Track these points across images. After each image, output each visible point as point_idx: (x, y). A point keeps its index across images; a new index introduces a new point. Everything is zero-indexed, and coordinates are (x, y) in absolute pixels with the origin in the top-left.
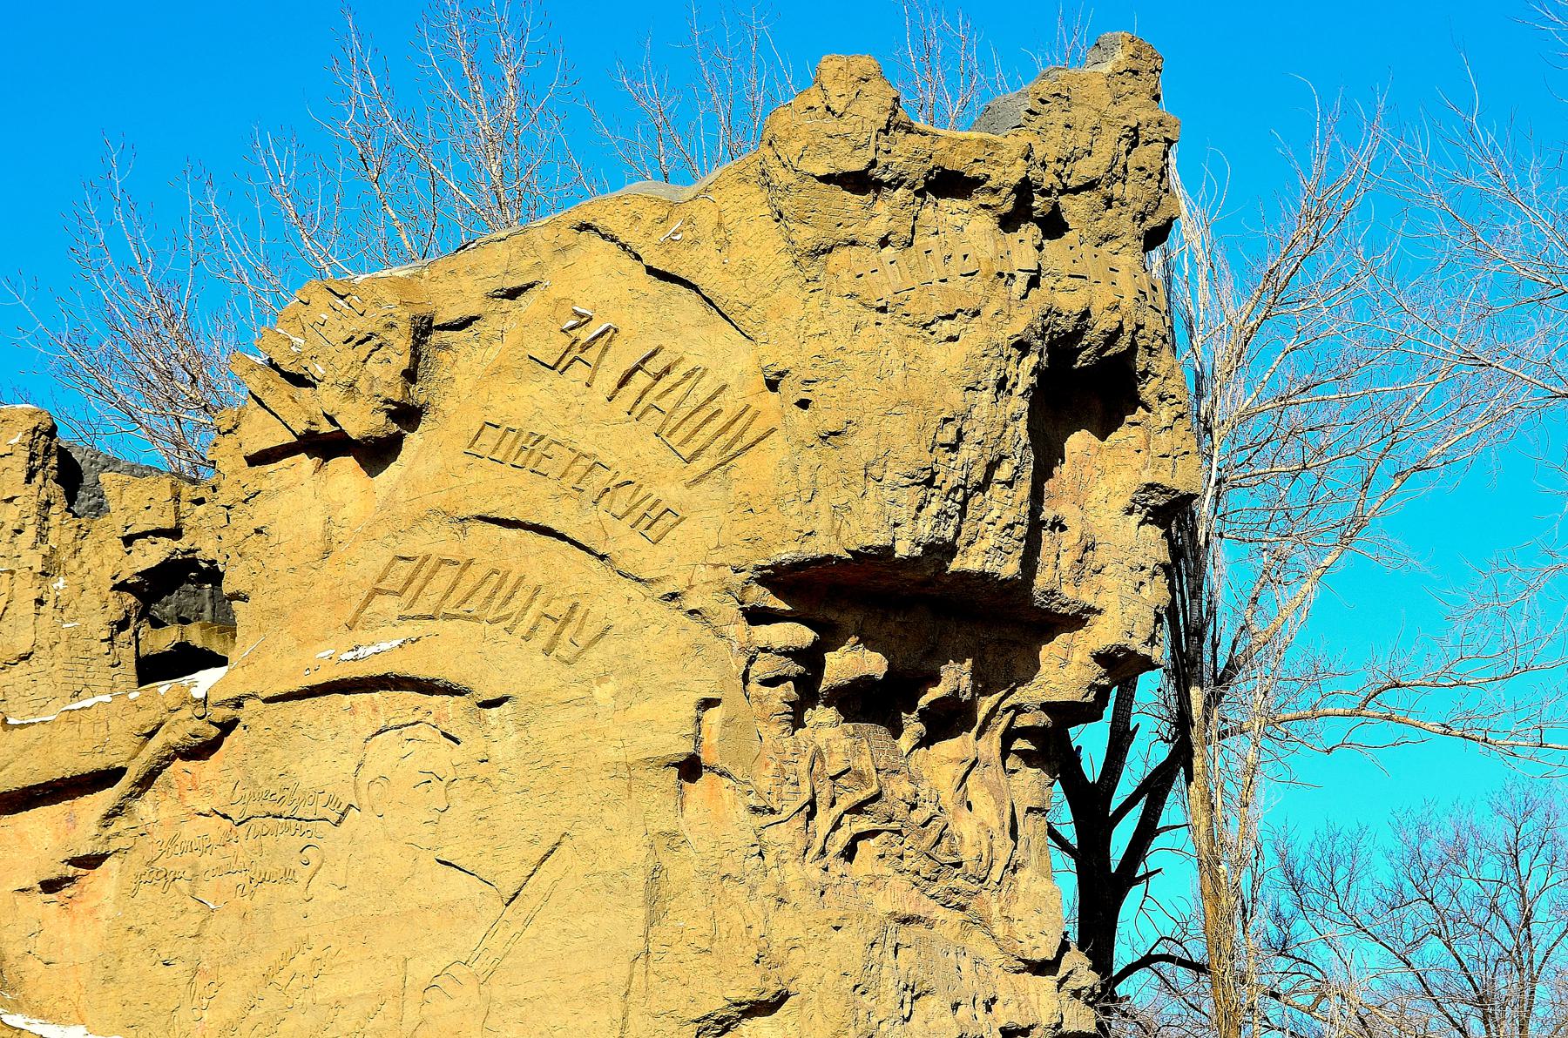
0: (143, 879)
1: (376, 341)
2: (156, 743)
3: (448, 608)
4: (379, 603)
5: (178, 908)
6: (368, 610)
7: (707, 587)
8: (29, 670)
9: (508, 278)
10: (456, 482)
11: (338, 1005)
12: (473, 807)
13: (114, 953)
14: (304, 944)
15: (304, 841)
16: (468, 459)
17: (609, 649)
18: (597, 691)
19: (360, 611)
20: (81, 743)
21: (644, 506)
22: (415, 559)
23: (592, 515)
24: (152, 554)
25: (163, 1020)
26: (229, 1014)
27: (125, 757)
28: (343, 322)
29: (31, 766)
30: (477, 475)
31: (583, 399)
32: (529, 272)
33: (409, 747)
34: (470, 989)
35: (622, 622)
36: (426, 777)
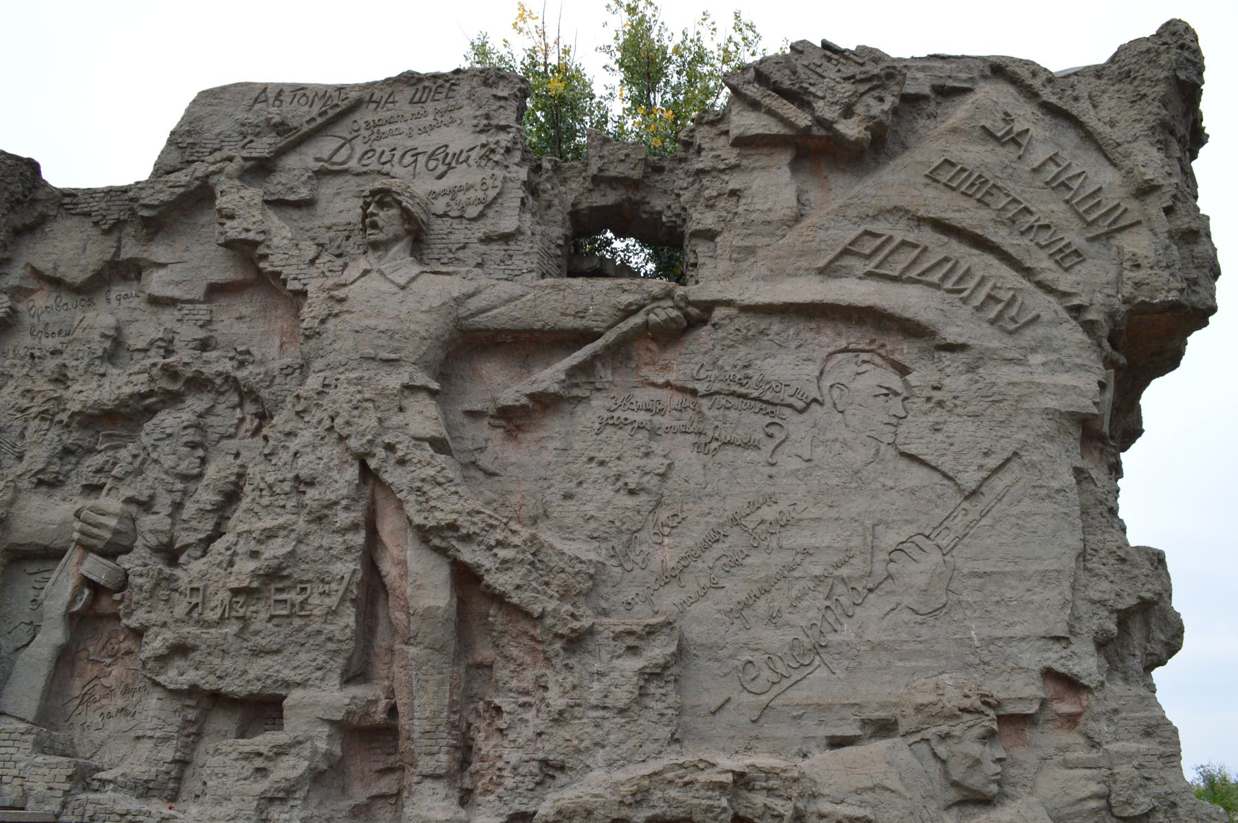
0: (610, 422)
1: (875, 83)
2: (638, 320)
3: (914, 274)
4: (848, 261)
5: (643, 449)
6: (837, 264)
7: (1103, 308)
8: (506, 247)
9: (951, 81)
10: (917, 193)
11: (806, 552)
12: (931, 419)
13: (574, 475)
14: (771, 500)
15: (768, 420)
16: (928, 181)
17: (1039, 331)
18: (1030, 357)
19: (831, 262)
20: (565, 307)
21: (1063, 243)
22: (880, 236)
23: (1025, 241)
24: (610, 198)
25: (625, 537)
26: (690, 543)
27: (604, 325)
28: (839, 66)
29: (514, 313)
30: (930, 193)
31: (1014, 165)
32: (965, 81)
33: (865, 367)
34: (936, 557)
35: (1046, 316)
36: (886, 391)
